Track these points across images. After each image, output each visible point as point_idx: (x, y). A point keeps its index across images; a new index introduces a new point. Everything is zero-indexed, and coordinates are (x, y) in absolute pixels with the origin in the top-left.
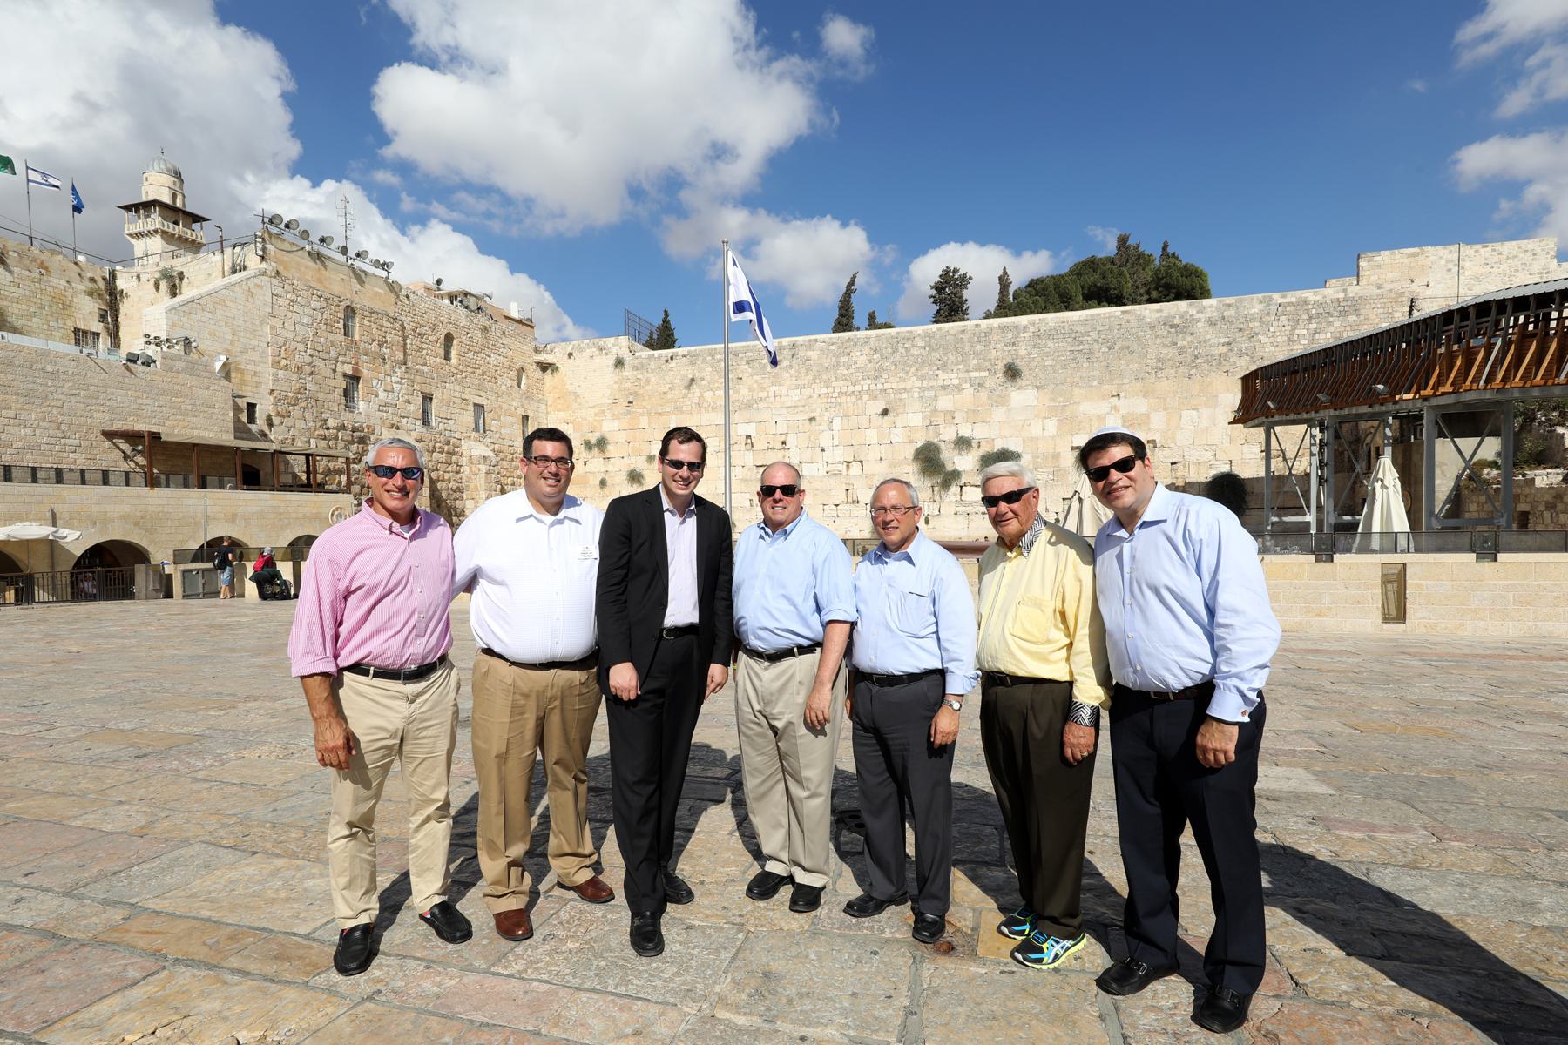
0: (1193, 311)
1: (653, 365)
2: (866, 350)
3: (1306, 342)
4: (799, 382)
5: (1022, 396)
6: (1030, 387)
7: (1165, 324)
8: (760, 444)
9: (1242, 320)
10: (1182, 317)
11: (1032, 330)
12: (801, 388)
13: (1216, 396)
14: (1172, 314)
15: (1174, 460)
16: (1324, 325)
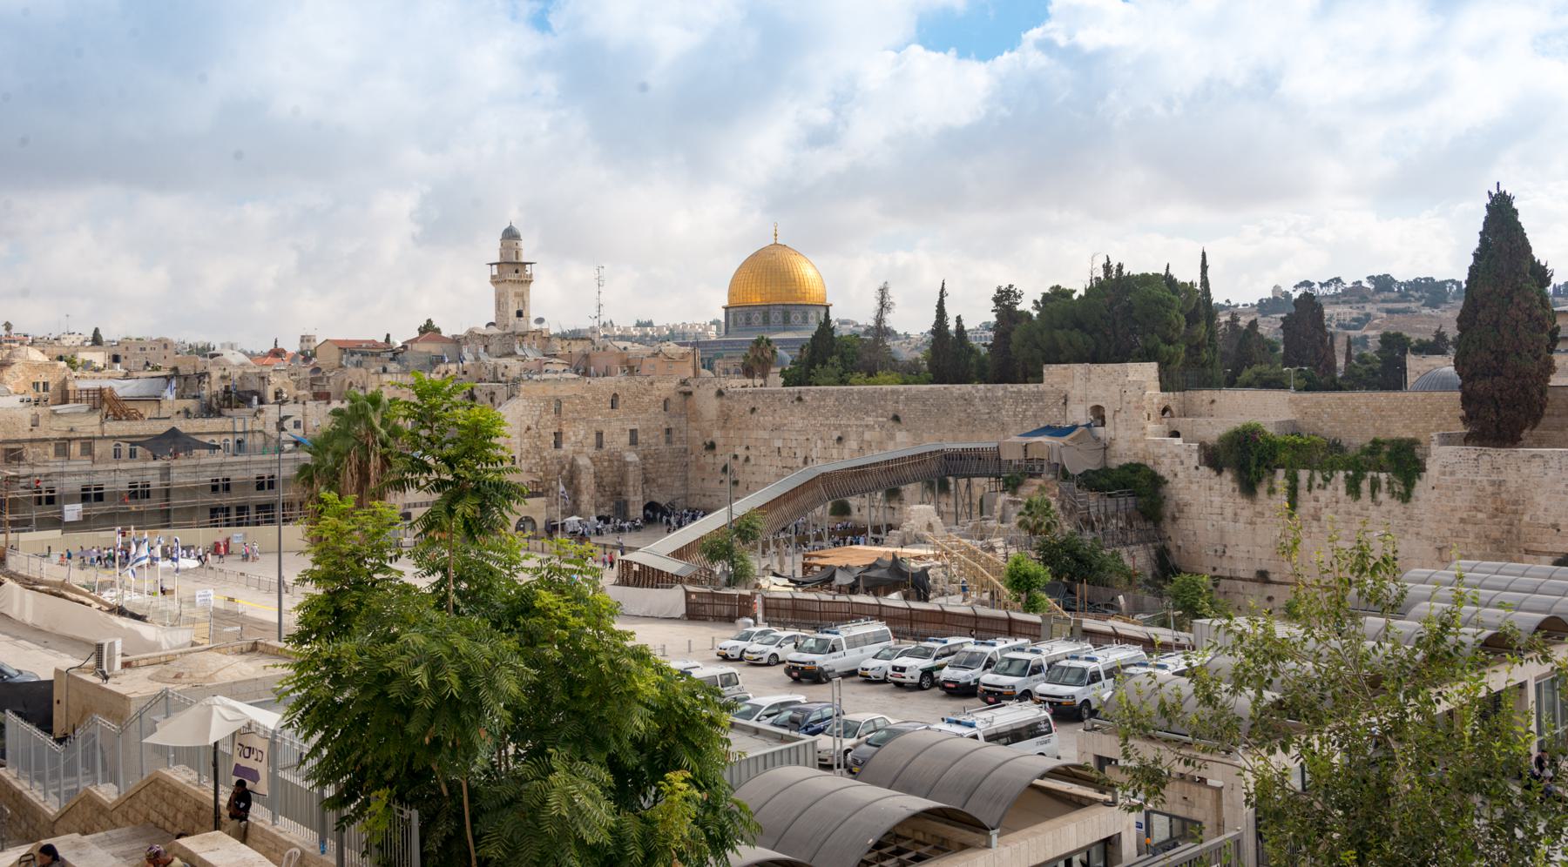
8: (784, 453)
10: (969, 393)
12: (803, 419)
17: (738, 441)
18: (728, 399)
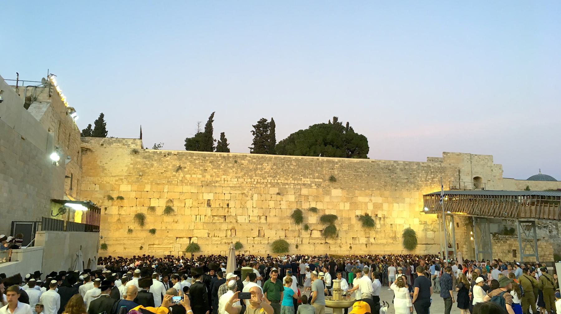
0: (395, 165)
1: (156, 157)
2: (271, 164)
3: (430, 181)
4: (237, 175)
5: (336, 192)
6: (339, 188)
7: (386, 168)
9: (411, 170)
10: (392, 166)
11: (339, 164)
13: (404, 198)
14: (389, 165)
15: (392, 223)
16: (436, 176)
17: (156, 195)
18: (146, 158)
